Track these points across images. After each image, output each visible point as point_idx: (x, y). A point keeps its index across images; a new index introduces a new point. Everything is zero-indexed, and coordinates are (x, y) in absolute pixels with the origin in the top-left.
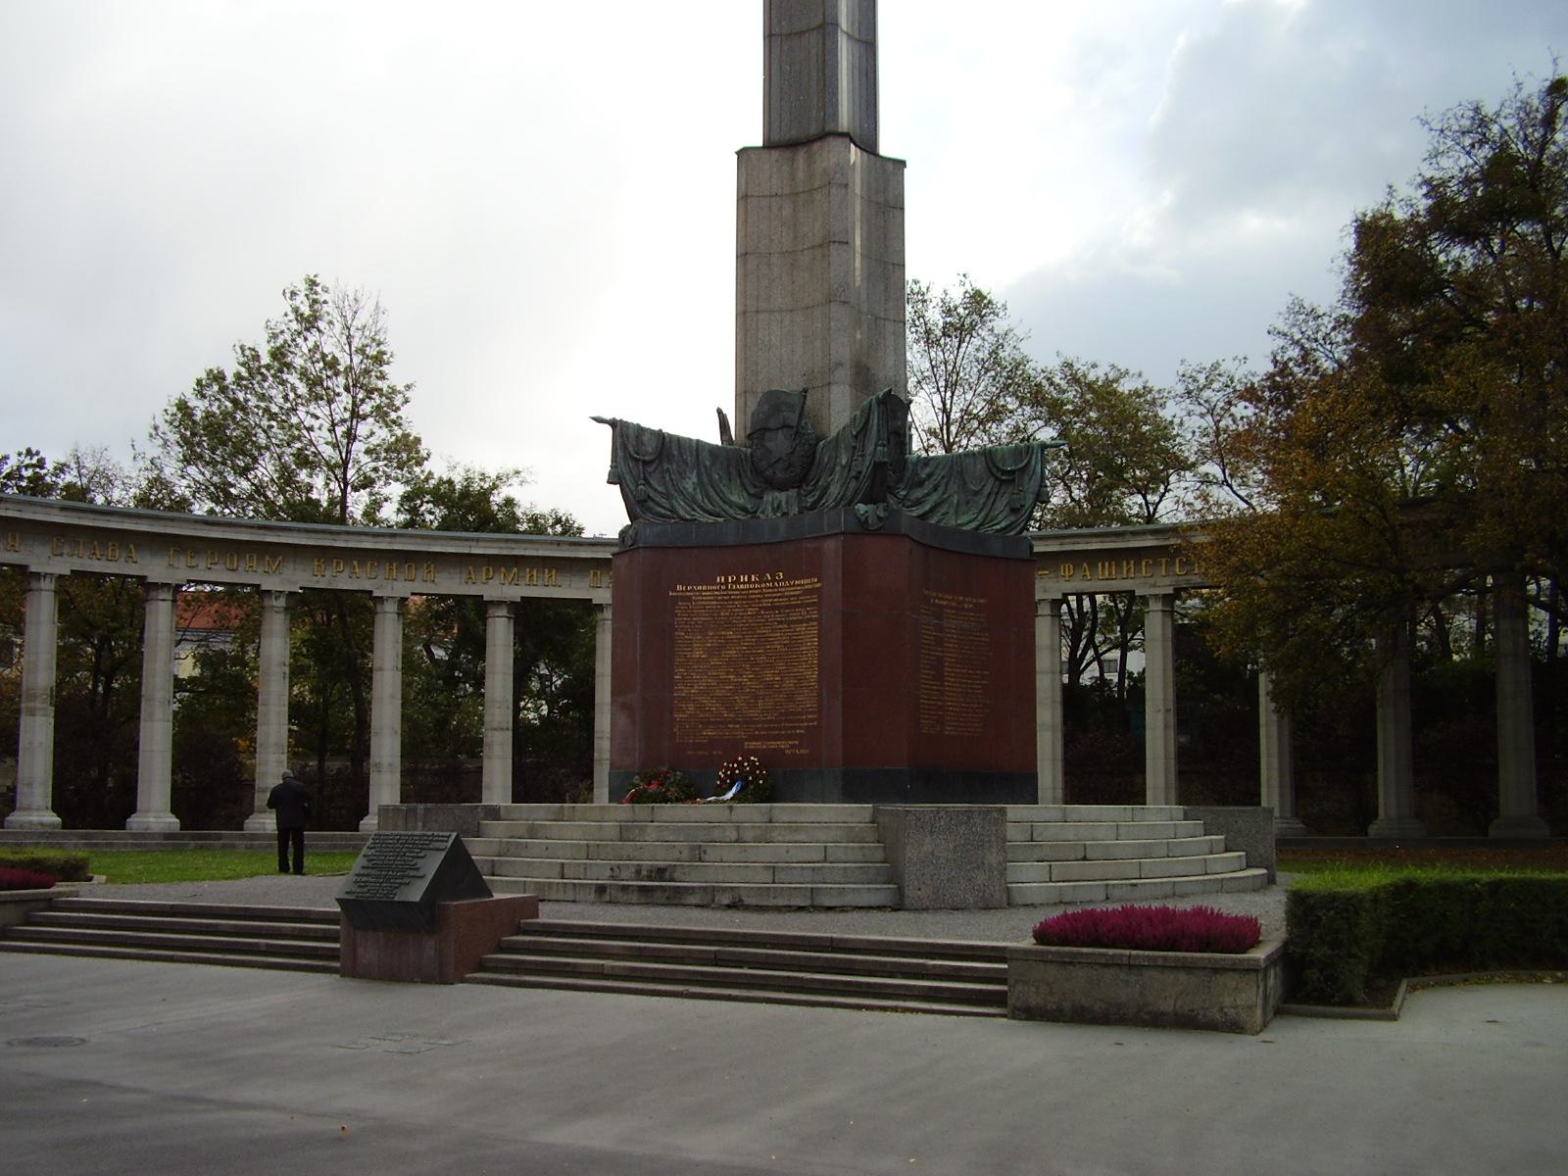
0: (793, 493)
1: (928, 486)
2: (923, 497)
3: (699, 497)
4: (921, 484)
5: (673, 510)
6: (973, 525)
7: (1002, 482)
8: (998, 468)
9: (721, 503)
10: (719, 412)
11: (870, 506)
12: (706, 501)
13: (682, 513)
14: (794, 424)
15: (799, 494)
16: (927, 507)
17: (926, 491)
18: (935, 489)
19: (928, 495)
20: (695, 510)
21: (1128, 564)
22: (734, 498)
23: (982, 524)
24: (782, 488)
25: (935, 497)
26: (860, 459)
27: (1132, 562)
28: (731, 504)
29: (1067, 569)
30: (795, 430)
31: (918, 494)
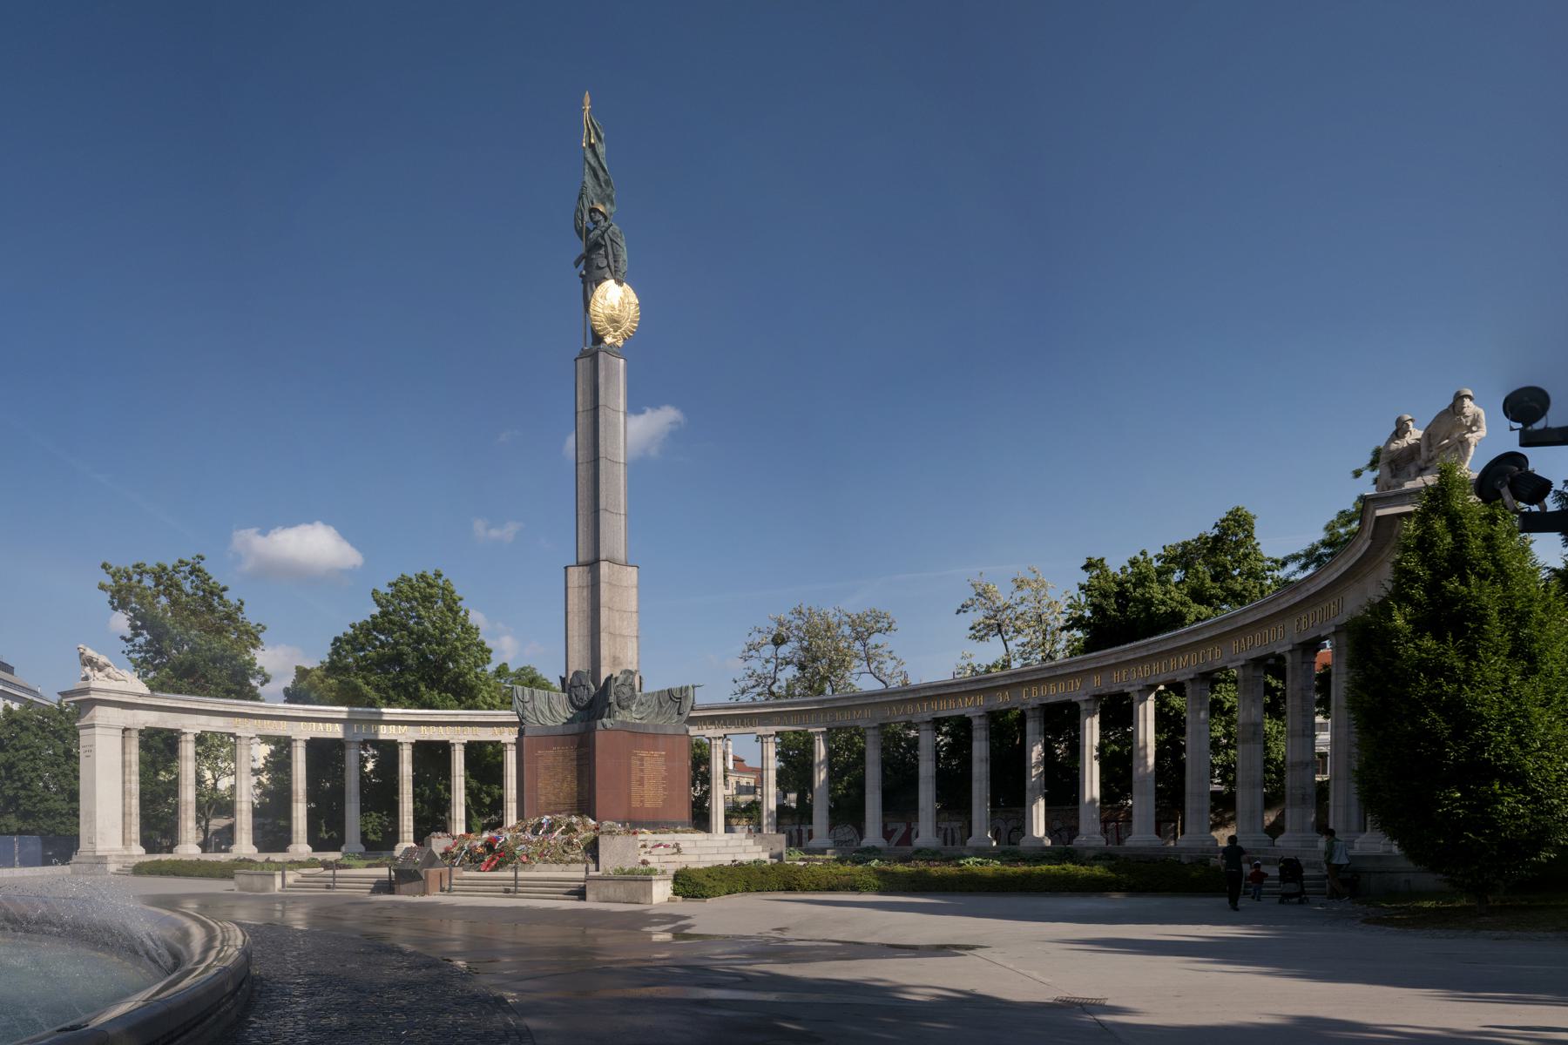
3: (548, 715)
4: (642, 704)
5: (538, 721)
10: (561, 677)
31: (641, 709)
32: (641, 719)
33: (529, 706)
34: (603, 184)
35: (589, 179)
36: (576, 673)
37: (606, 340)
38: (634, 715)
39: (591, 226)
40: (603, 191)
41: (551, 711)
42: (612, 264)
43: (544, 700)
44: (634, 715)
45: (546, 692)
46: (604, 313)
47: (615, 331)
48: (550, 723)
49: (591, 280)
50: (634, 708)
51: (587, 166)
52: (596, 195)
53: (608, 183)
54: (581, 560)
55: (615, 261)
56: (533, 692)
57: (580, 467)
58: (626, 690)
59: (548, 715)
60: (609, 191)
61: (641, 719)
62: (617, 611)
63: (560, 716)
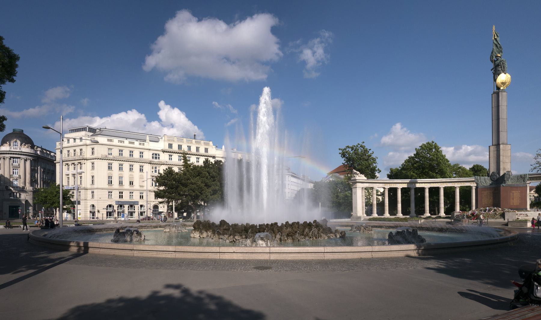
33: (479, 181)
34: (499, 48)
35: (495, 48)
36: (493, 173)
39: (496, 59)
40: (499, 50)
41: (485, 182)
42: (503, 69)
47: (504, 86)
48: (485, 185)
49: (496, 73)
51: (494, 44)
52: (497, 51)
53: (501, 47)
54: (494, 144)
55: (504, 68)
56: (480, 178)
57: (493, 121)
60: (501, 50)
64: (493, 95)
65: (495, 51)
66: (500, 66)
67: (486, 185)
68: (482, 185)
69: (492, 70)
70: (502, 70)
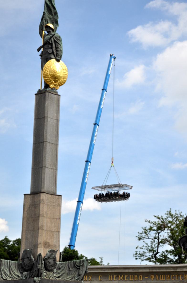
0: (29, 272)
1: (61, 269)
2: (60, 272)
3: (8, 274)
4: (60, 269)
5: (2, 277)
6: (70, 279)
7: (78, 268)
8: (77, 265)
9: (13, 275)
11: (38, 278)
12: (10, 275)
13: (4, 278)
14: (30, 257)
15: (30, 273)
16: (60, 275)
17: (61, 271)
18: (63, 270)
19: (61, 271)
20: (7, 277)
21: (168, 276)
22: (17, 274)
23: (72, 278)
24: (27, 271)
25: (62, 272)
26: (36, 267)
27: (169, 275)
28: (15, 275)
29: (152, 277)
30: (30, 258)
31: (59, 271)
32: (58, 277)
34: (53, 14)
37: (50, 86)
38: (55, 275)
42: (55, 51)
43: (6, 265)
44: (55, 275)
45: (9, 261)
46: (50, 74)
48: (9, 279)
50: (55, 271)
51: (46, 6)
52: (50, 19)
53: (56, 13)
55: (57, 51)
58: (51, 261)
59: (8, 274)
61: (58, 277)
62: (49, 218)
63: (15, 275)
64: (38, 96)
65: (47, 18)
66: (50, 46)
67: (10, 279)
68: (3, 280)
69: (39, 50)
70: (53, 53)
